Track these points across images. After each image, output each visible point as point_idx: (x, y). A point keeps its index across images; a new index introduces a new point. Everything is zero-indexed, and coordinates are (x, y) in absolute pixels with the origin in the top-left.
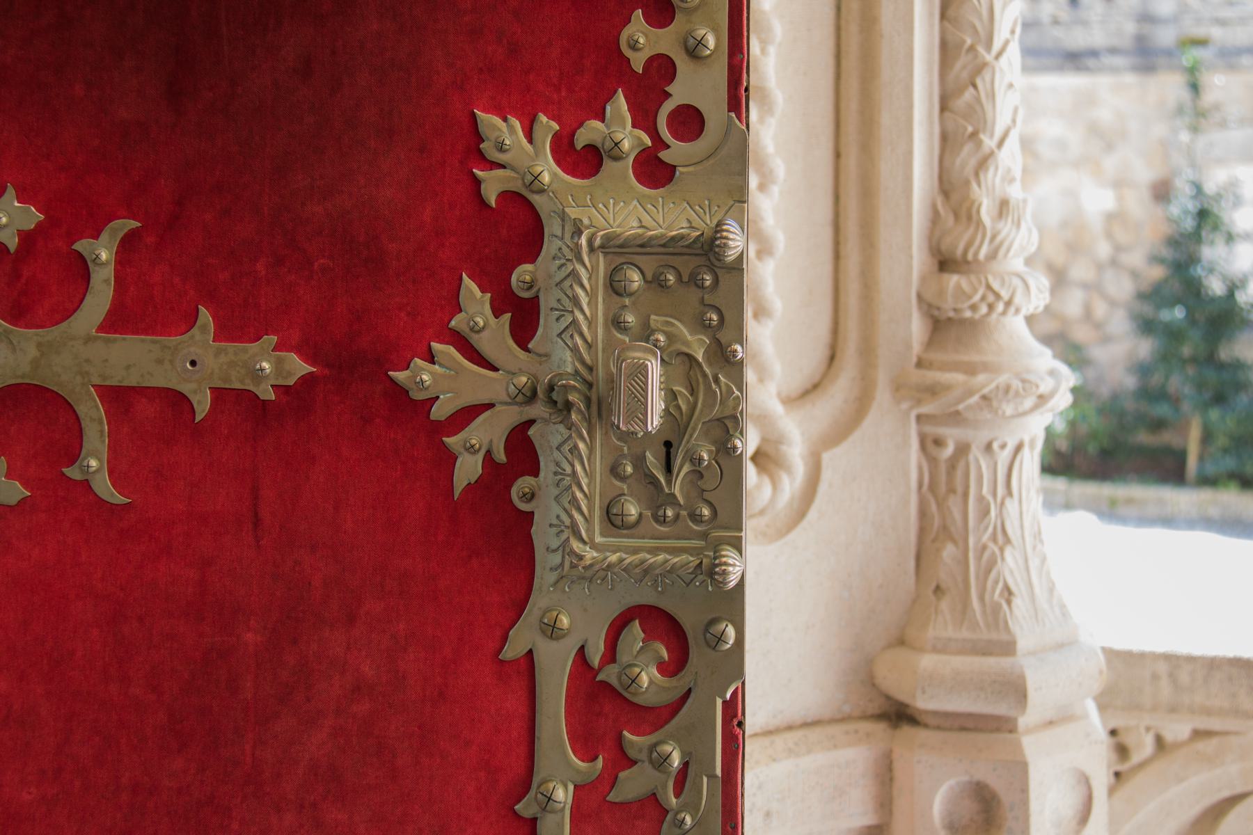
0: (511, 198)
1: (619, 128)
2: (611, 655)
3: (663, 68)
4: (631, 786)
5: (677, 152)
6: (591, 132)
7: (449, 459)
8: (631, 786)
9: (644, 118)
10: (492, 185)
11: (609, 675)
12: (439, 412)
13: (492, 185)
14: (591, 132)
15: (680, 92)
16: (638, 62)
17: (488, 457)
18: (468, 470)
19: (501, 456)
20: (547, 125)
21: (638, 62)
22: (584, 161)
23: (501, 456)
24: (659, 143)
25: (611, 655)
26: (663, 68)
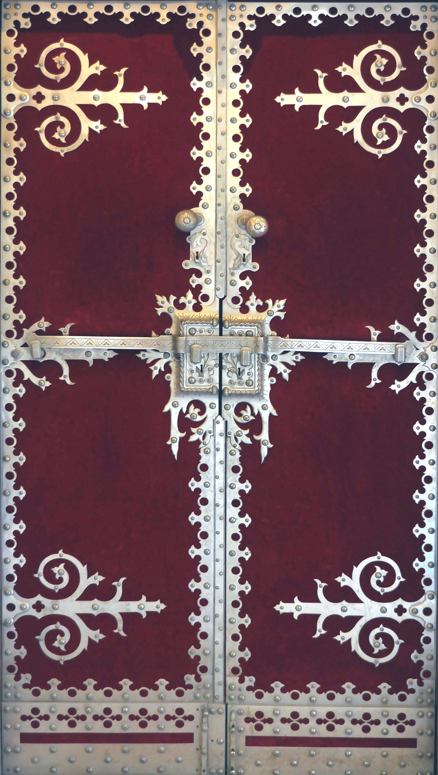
0: (163, 314)
1: (189, 298)
2: (187, 412)
3: (199, 287)
4: (193, 438)
5: (203, 304)
6: (182, 300)
7: (151, 371)
8: (193, 438)
9: (195, 297)
10: (160, 311)
11: (188, 416)
12: (149, 362)
13: (160, 311)
14: (182, 300)
15: (204, 292)
16: (194, 286)
17: (160, 370)
18: (155, 373)
19: (163, 369)
20: (173, 298)
21: (194, 286)
22: (182, 307)
23: (163, 369)
24: (199, 303)
25: (187, 412)
26: (199, 287)
